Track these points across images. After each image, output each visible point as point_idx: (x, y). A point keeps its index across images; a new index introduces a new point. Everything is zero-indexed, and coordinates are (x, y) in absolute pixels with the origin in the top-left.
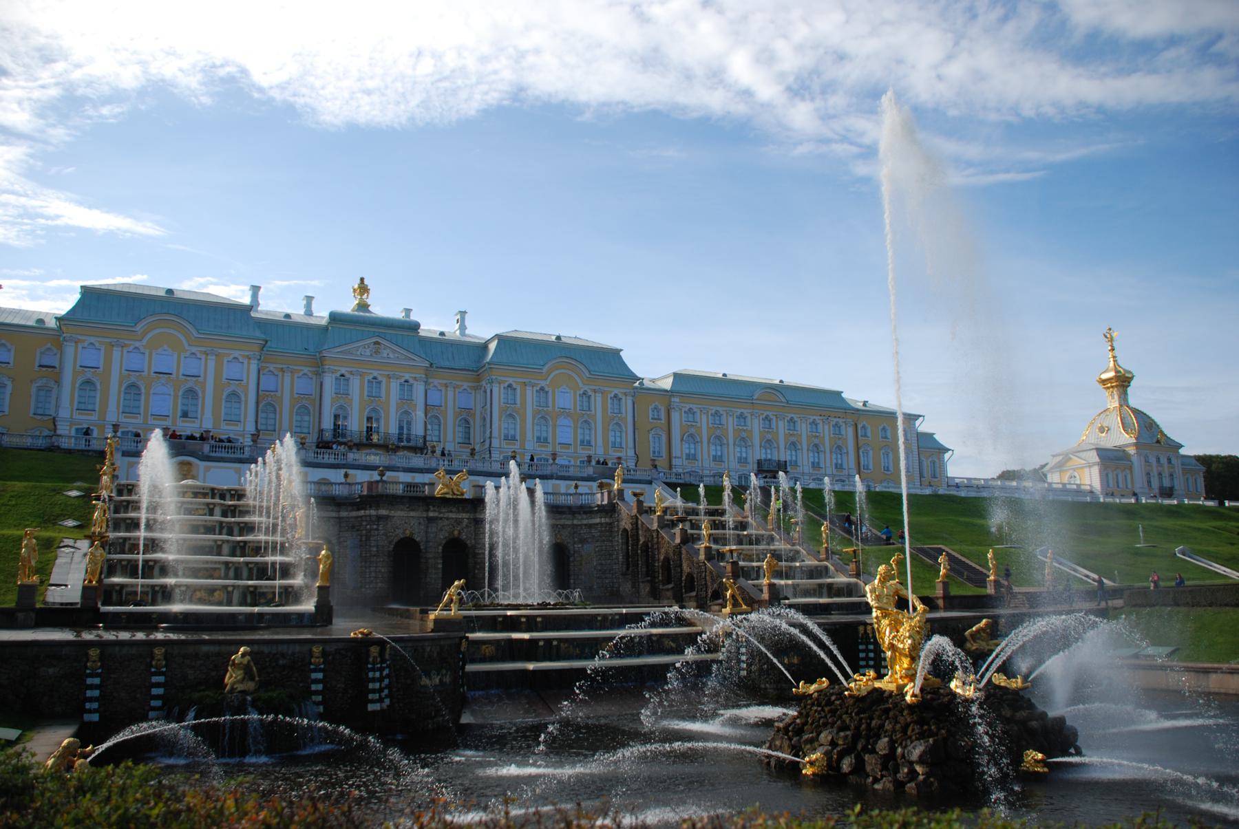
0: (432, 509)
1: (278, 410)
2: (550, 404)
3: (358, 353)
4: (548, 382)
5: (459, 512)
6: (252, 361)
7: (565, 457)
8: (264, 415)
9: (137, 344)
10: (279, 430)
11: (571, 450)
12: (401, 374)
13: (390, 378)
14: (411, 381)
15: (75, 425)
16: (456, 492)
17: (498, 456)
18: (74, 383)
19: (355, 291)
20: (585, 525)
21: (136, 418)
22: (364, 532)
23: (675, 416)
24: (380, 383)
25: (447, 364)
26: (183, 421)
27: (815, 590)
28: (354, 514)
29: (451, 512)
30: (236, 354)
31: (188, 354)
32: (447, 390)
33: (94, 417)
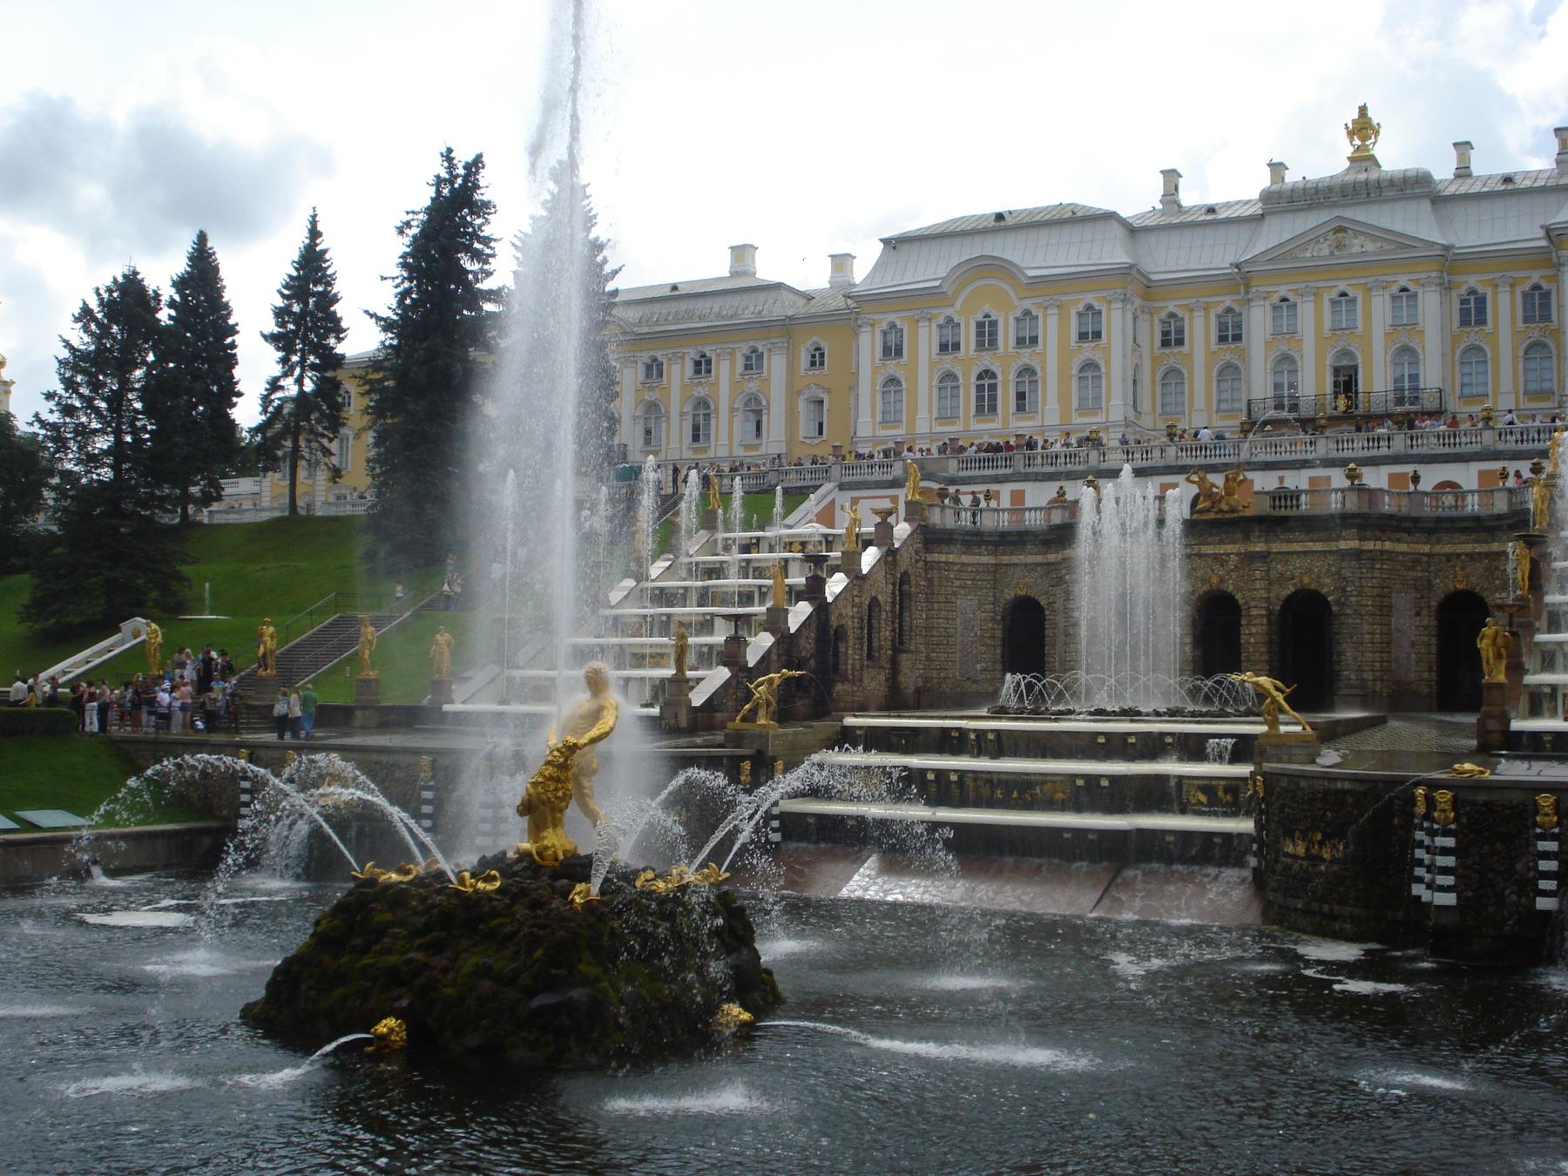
1: (1186, 376)
3: (1308, 254)
5: (1222, 542)
6: (1114, 306)
9: (949, 312)
10: (1190, 412)
12: (1392, 278)
13: (1370, 289)
14: (1412, 288)
15: (881, 443)
18: (873, 385)
19: (1351, 134)
21: (955, 423)
24: (1354, 300)
26: (1018, 419)
30: (1089, 298)
31: (1018, 314)
32: (1495, 294)
33: (900, 432)
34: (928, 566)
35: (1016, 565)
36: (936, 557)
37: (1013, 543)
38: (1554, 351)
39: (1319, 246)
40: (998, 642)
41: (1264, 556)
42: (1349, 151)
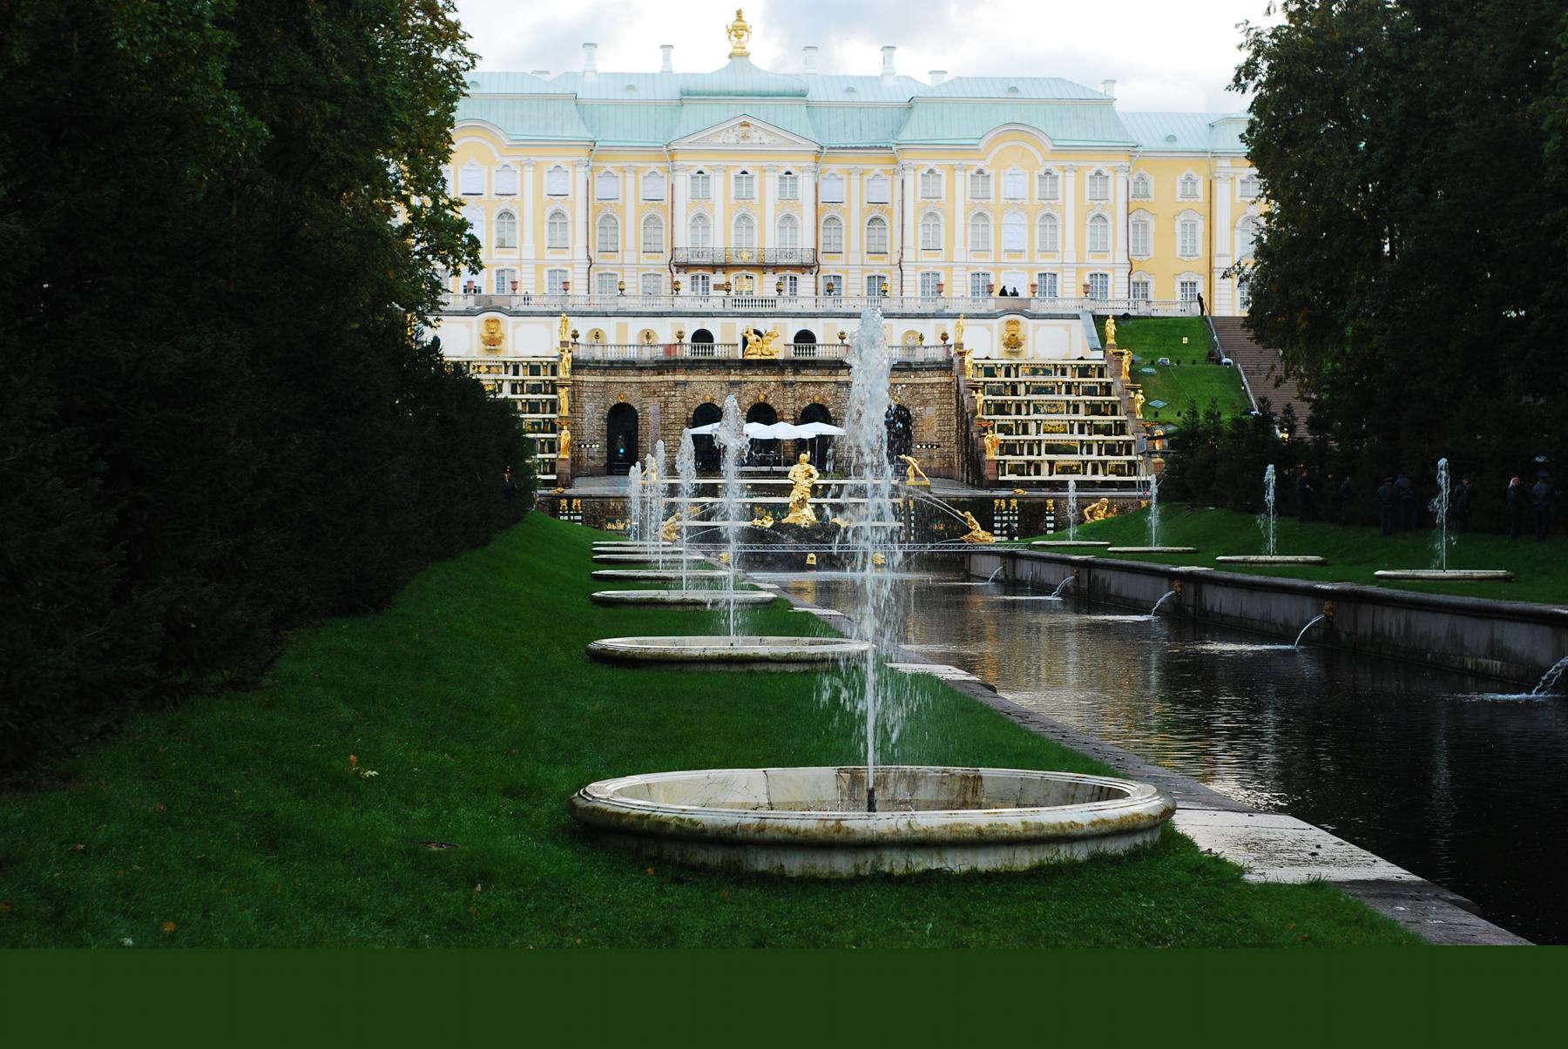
0: (733, 372)
2: (992, 195)
3: (721, 141)
4: (989, 161)
5: (765, 374)
6: (578, 169)
7: (1014, 270)
8: (603, 232)
10: (623, 251)
11: (1025, 258)
16: (765, 352)
17: (913, 273)
19: (730, 32)
20: (928, 384)
22: (663, 398)
23: (1223, 191)
25: (850, 142)
26: (499, 252)
27: (1078, 467)
28: (655, 378)
29: (756, 374)
30: (558, 161)
34: (575, 383)
35: (619, 383)
36: (578, 378)
37: (617, 368)
38: (888, 224)
39: (728, 135)
40: (605, 433)
41: (792, 384)
42: (731, 50)
